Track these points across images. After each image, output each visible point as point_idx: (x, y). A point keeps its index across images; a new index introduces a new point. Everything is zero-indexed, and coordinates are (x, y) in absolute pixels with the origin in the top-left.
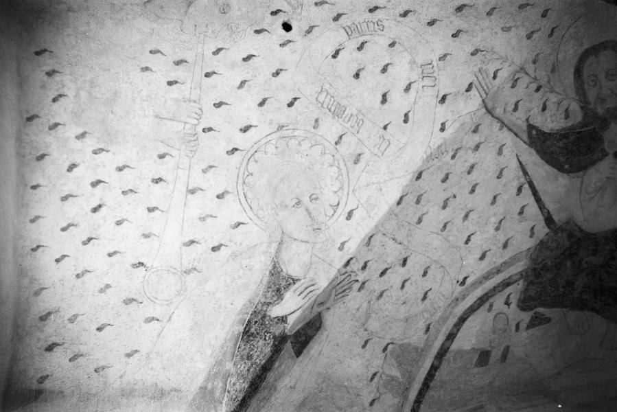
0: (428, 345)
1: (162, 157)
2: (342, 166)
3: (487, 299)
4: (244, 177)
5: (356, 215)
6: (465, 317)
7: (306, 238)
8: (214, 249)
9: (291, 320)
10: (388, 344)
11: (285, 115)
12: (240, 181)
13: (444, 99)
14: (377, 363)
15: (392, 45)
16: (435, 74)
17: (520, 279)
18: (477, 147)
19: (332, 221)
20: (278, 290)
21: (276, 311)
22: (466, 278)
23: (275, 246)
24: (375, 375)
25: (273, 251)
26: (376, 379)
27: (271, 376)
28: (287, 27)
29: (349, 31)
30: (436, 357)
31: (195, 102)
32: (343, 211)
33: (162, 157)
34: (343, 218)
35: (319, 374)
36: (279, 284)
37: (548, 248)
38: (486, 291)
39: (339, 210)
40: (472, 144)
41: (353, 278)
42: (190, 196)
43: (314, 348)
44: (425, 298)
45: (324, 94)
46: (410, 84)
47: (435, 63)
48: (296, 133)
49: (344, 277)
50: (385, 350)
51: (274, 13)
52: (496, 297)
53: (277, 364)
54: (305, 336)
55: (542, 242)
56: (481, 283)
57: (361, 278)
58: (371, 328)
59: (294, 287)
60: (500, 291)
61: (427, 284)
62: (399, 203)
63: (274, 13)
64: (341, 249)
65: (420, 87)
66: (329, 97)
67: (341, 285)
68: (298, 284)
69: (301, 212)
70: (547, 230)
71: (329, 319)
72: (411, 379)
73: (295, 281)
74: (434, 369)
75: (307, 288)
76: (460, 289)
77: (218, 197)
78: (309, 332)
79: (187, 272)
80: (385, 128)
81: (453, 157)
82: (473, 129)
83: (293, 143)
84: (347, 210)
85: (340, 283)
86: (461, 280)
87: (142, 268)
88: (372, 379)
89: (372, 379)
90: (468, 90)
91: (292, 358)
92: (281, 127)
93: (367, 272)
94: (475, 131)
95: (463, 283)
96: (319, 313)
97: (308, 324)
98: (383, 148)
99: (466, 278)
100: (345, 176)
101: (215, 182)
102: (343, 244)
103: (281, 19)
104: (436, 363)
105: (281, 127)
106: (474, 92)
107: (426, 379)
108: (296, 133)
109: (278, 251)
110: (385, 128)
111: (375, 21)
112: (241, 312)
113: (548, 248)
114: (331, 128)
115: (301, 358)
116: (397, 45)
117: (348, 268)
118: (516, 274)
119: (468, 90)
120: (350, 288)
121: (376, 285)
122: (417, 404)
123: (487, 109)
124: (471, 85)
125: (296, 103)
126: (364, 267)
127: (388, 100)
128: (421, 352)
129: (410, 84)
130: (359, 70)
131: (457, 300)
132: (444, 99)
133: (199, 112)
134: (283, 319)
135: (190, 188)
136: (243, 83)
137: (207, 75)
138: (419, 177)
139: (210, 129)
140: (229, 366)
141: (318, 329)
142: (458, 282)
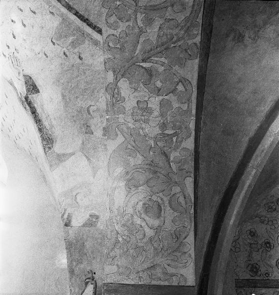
0: (62, 15)
10: (52, 41)
14: (59, 50)
24: (64, 53)
26: (67, 53)
30: (70, 11)
35: (54, 83)
43: (39, 83)
44: (34, 13)
49: (10, 59)
50: (54, 44)
53: (36, 105)
57: (13, 50)
61: (27, 12)
71: (28, 72)
72: (78, 29)
74: (76, 14)
88: (66, 56)
89: (66, 56)
93: (11, 47)
96: (24, 76)
97: (26, 83)
104: (74, 12)
107: (81, 20)
117: (7, 56)
122: (96, 28)
128: (64, 19)
141: (30, 78)
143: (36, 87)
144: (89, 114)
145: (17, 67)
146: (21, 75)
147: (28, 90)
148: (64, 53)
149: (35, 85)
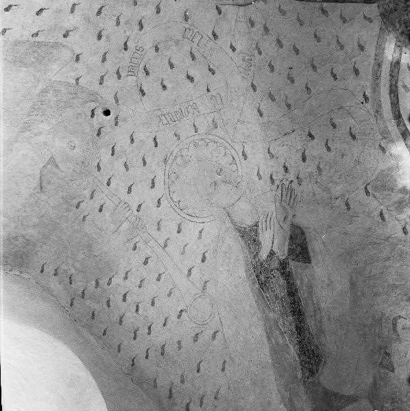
1: (135, 248)
2: (210, 137)
3: (397, 87)
4: (178, 207)
5: (248, 150)
6: (397, 113)
7: (236, 197)
8: (203, 261)
9: (275, 249)
10: (366, 188)
11: (160, 153)
12: (179, 211)
13: (214, 35)
15: (157, 49)
16: (195, 30)
17: (401, 50)
18: (266, 29)
19: (240, 170)
20: (254, 240)
21: (264, 254)
22: (364, 95)
23: (227, 220)
25: (229, 224)
27: (303, 294)
28: (107, 113)
29: (132, 72)
31: (119, 203)
32: (239, 157)
33: (135, 248)
34: (243, 161)
36: (250, 236)
37: (391, 12)
38: (388, 85)
39: (237, 159)
40: (262, 31)
41: (287, 183)
42: (167, 249)
43: (315, 246)
45: (163, 118)
46: (191, 53)
47: (187, 26)
48: (174, 154)
51: (93, 115)
52: (400, 77)
53: (298, 282)
54: (299, 247)
55: (382, 15)
56: (377, 85)
57: (291, 177)
58: (338, 194)
59: (260, 231)
60: (398, 73)
62: (261, 115)
63: (93, 115)
64: (260, 178)
65: (198, 47)
66: (166, 116)
67: (284, 195)
68: (260, 224)
69: (222, 187)
70: (375, 5)
71: (302, 221)
73: (256, 225)
75: (266, 221)
76: (369, 106)
77: (179, 232)
78: (298, 241)
79: (204, 288)
80: (208, 90)
81: (260, 53)
82: (249, 25)
83: (179, 159)
84: (241, 154)
85: (282, 195)
86: (362, 99)
87: (183, 313)
90: (220, 13)
91: (306, 267)
92: (165, 161)
93: (291, 171)
94: (252, 24)
95: (366, 99)
97: (291, 238)
98: (219, 102)
99: (364, 95)
100: (221, 141)
101: (170, 228)
102: (258, 174)
103: (99, 112)
105: (165, 161)
106: (223, 9)
108: (174, 154)
109: (232, 221)
110: (208, 90)
111: (134, 50)
112: (249, 276)
113: (391, 12)
114: (185, 130)
115: (313, 261)
116: (159, 47)
117: (277, 182)
118: (395, 51)
119: (220, 13)
120: (293, 190)
121: (310, 167)
123: (241, 5)
124: (217, 8)
125: (158, 140)
126: (286, 169)
127: (193, 76)
129: (191, 53)
130: (162, 83)
131: (377, 112)
132: (214, 35)
133: (126, 205)
134: (272, 254)
135: (163, 245)
136: (126, 165)
137: (108, 184)
138: (254, 87)
139: (140, 206)
140: (271, 315)
141: (303, 233)
142: (362, 103)
143: (307, 253)
144: (395, 330)
145: (288, 207)
146: (289, 223)
147: (291, 251)
148: (381, 214)
149: (306, 248)
